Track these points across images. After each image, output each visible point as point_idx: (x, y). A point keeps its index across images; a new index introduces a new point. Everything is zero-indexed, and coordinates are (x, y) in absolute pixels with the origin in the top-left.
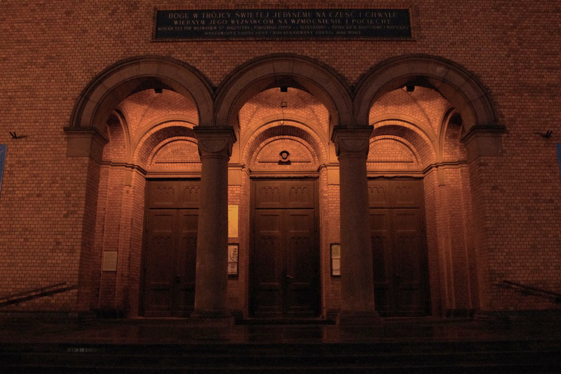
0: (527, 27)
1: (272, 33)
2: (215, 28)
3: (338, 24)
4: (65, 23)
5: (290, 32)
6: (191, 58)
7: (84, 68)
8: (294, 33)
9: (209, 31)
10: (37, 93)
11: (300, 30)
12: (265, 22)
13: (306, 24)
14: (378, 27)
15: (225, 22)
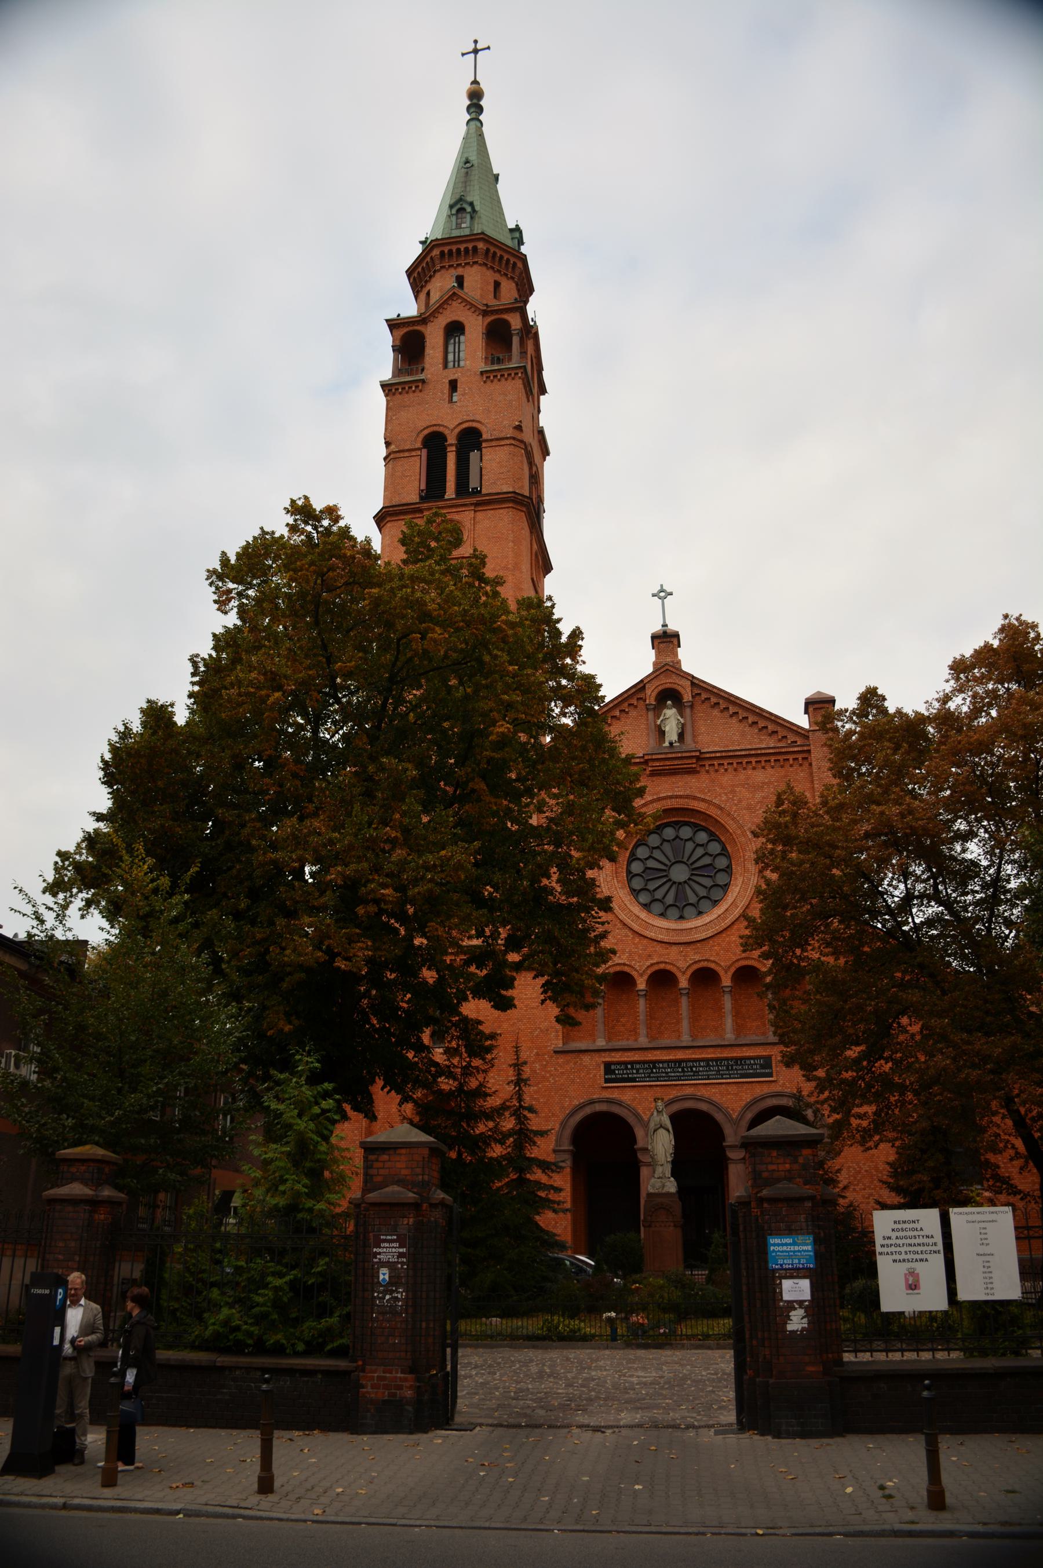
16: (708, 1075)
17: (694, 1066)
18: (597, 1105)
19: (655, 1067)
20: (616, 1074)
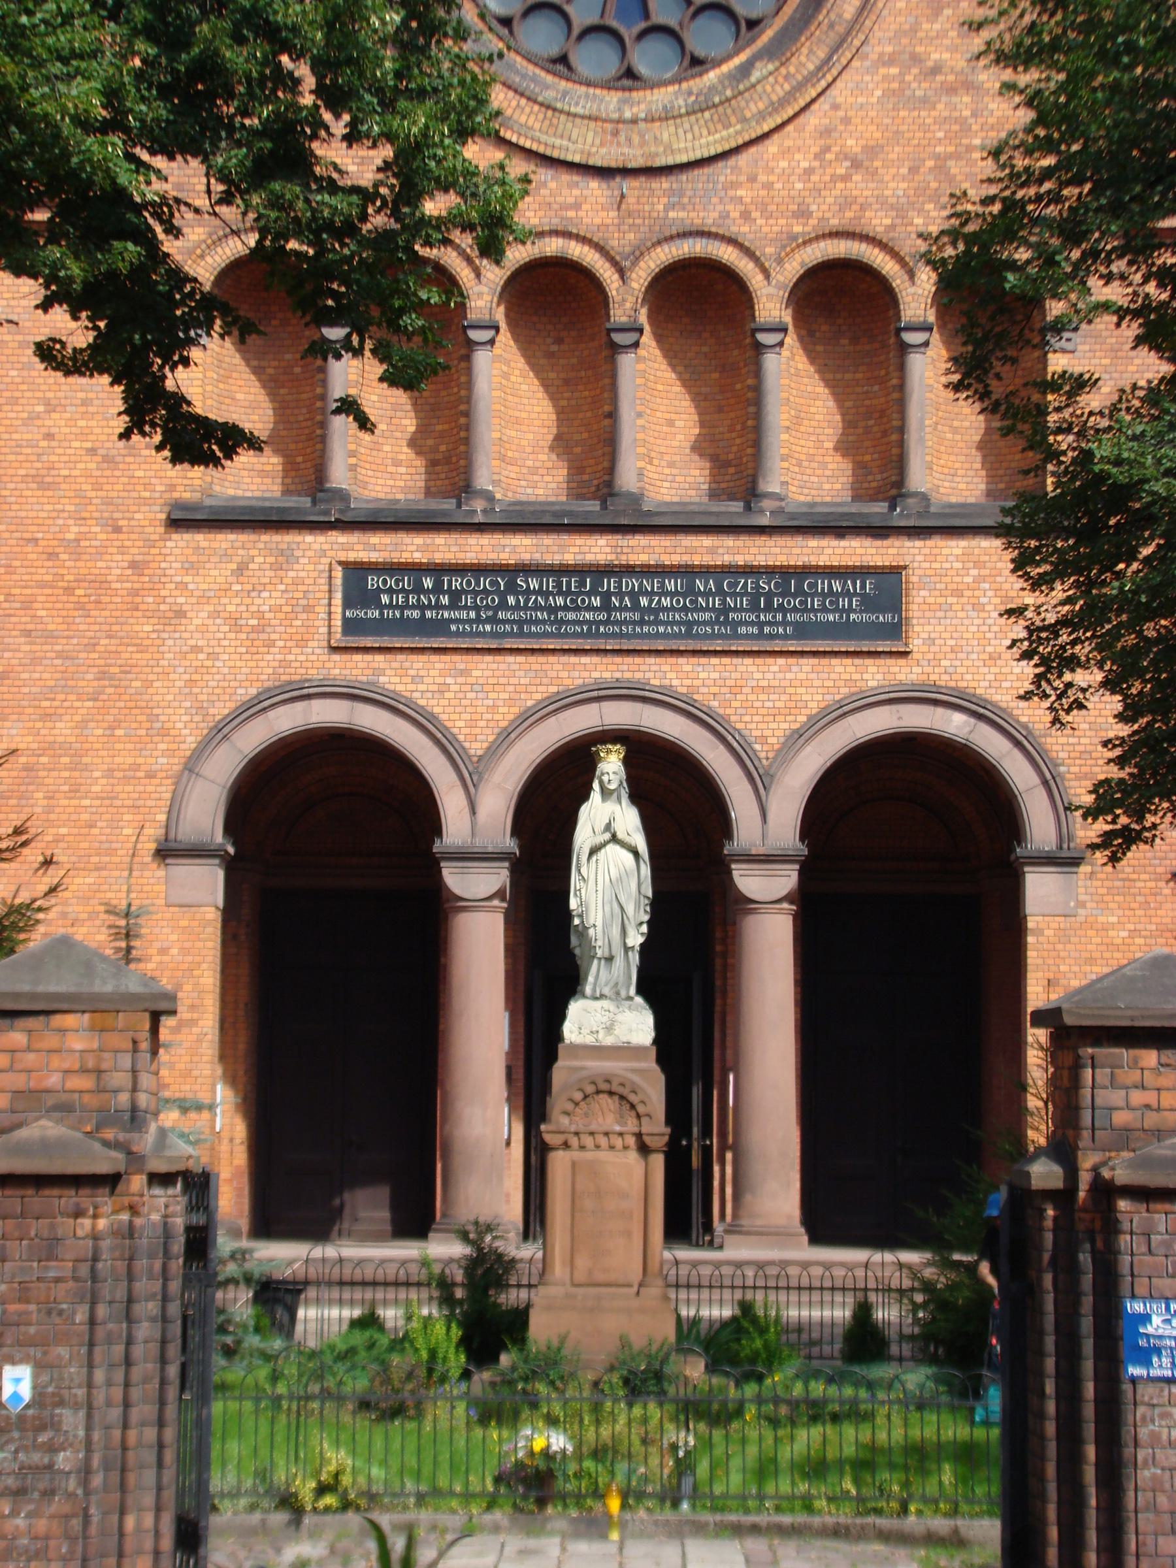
1: (598, 629)
2: (473, 615)
3: (742, 610)
4: (135, 593)
5: (638, 629)
6: (422, 687)
7: (188, 704)
8: (645, 629)
9: (457, 621)
10: (85, 760)
11: (657, 622)
12: (583, 601)
13: (672, 609)
14: (831, 618)
15: (493, 600)
16: (689, 624)
18: (316, 704)
19: (512, 588)
20: (381, 607)
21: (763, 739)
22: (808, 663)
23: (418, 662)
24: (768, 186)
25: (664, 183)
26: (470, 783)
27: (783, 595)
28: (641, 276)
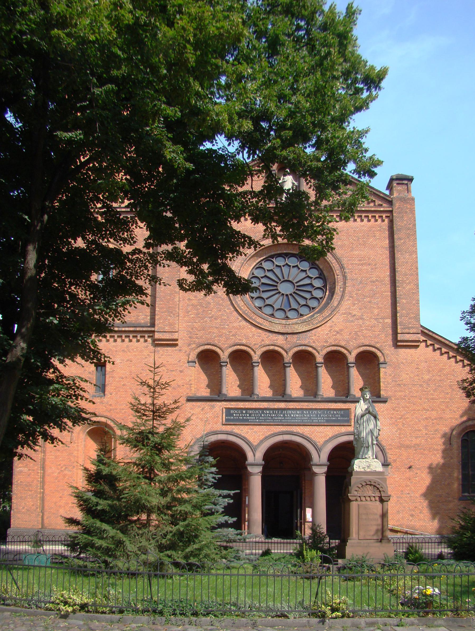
0: (407, 418)
16: (303, 420)
17: (292, 413)
19: (263, 413)
21: (319, 442)
22: (329, 427)
23: (242, 427)
24: (319, 336)
25: (296, 336)
26: (254, 450)
27: (324, 414)
28: (291, 353)
